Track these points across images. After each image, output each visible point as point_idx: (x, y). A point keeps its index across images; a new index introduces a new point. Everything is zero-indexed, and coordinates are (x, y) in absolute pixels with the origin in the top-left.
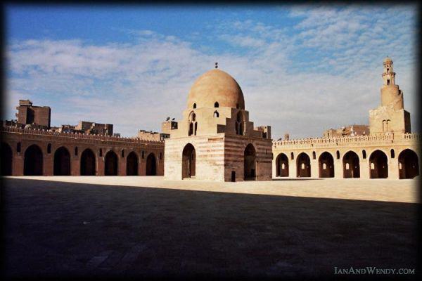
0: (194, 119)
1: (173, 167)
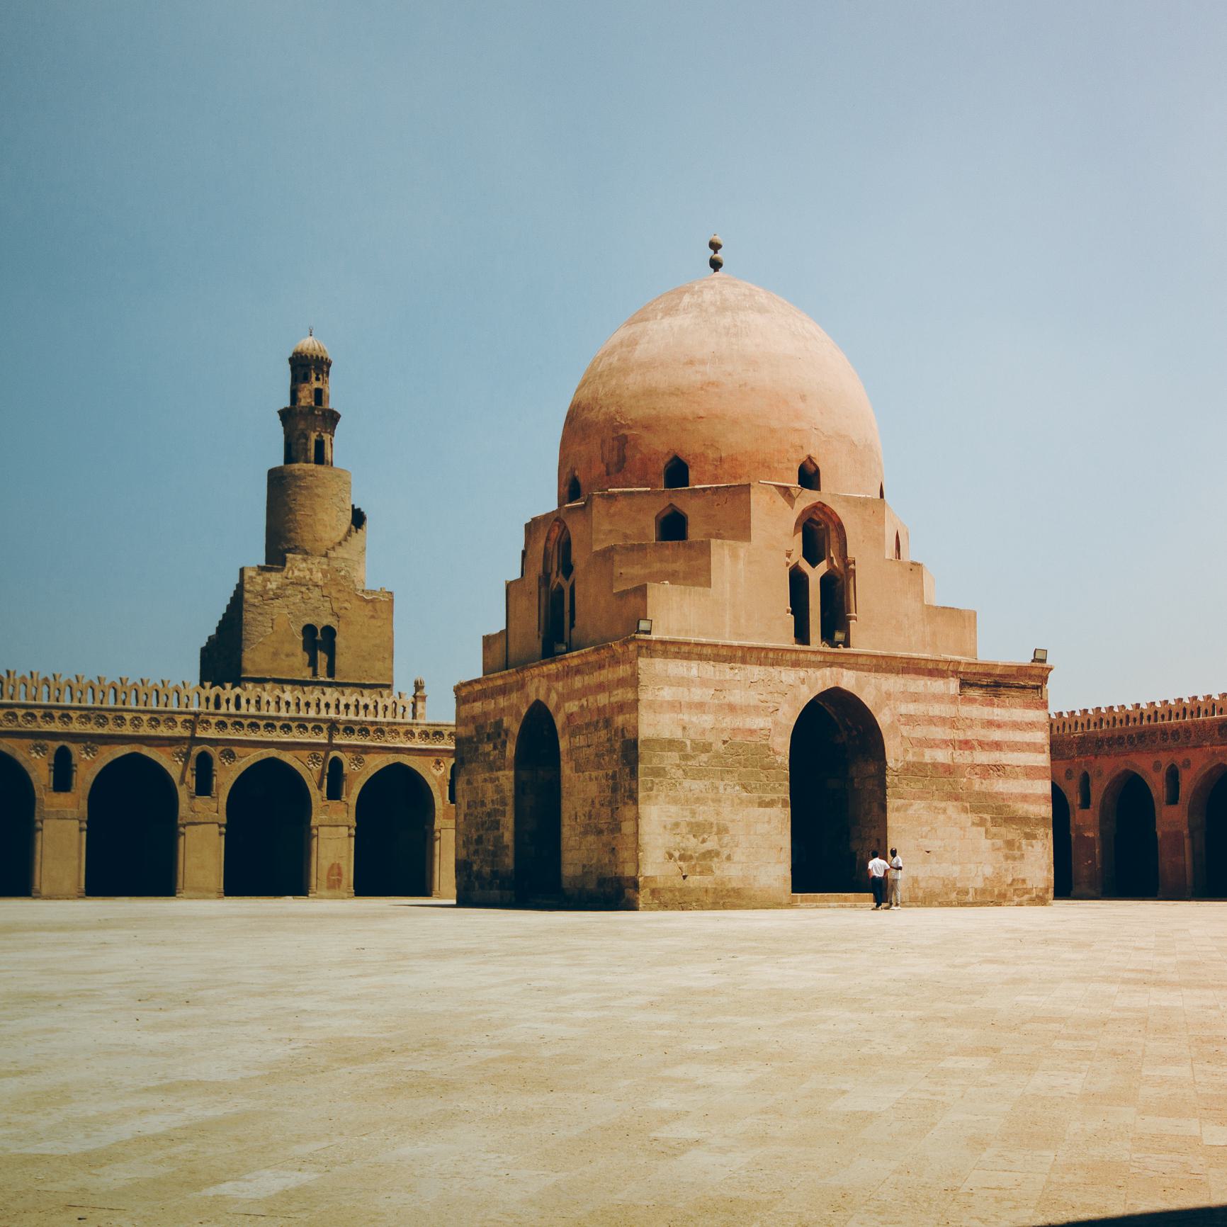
0: (813, 552)
1: (722, 830)
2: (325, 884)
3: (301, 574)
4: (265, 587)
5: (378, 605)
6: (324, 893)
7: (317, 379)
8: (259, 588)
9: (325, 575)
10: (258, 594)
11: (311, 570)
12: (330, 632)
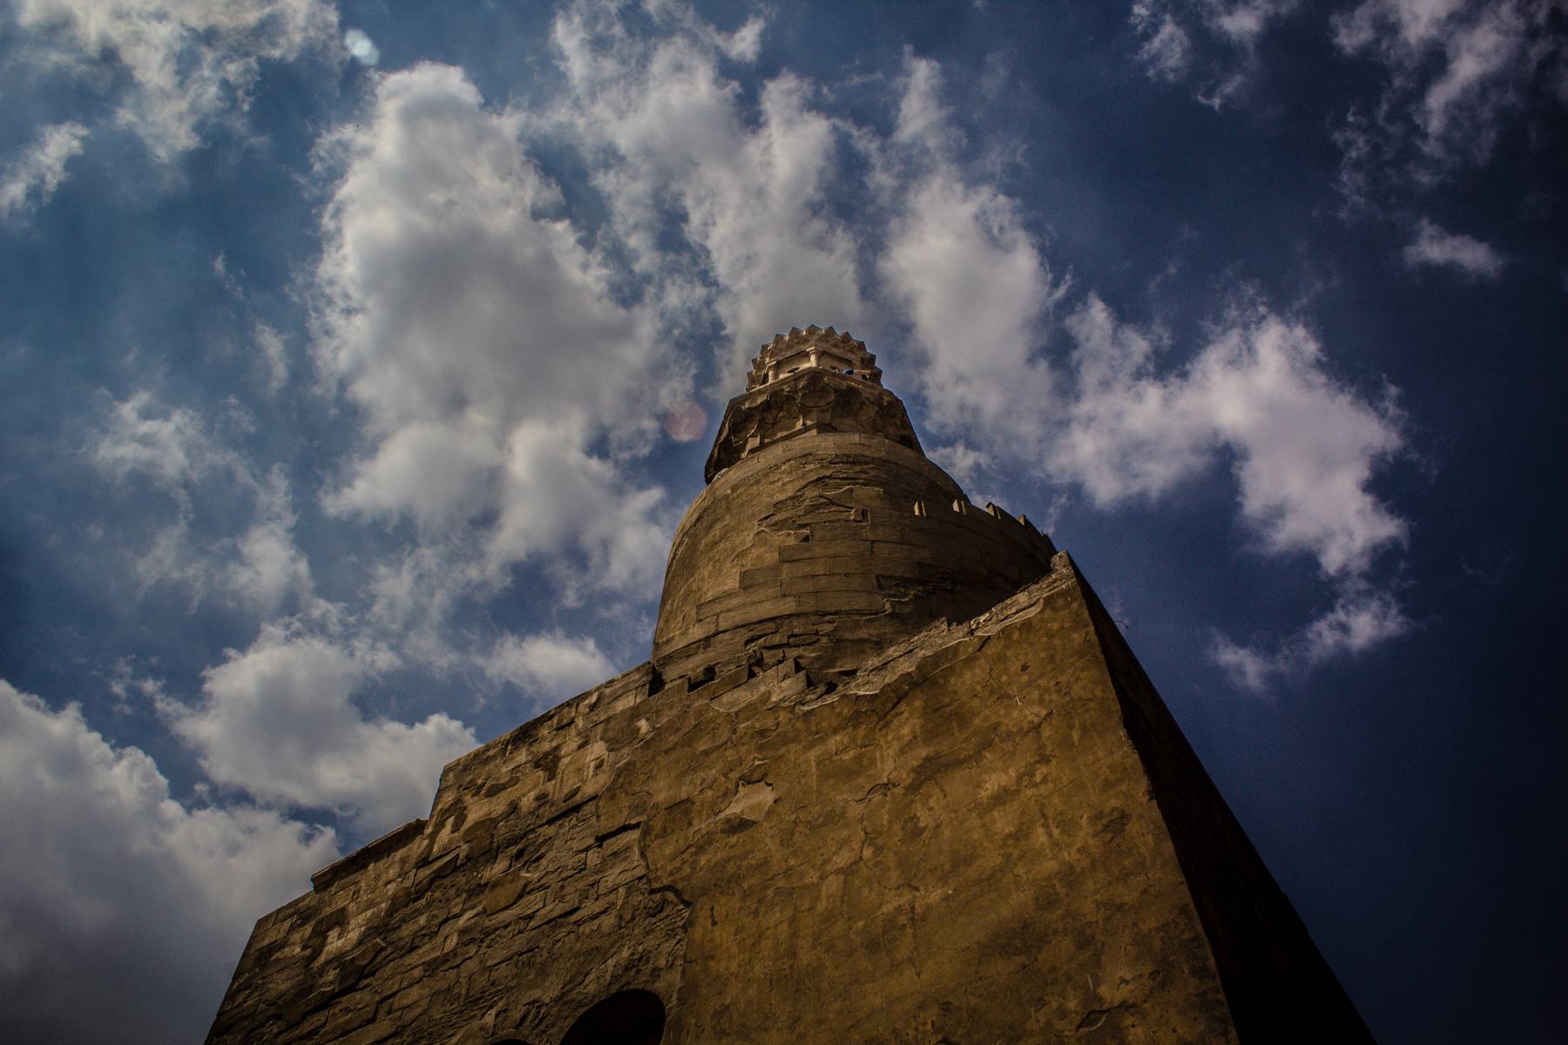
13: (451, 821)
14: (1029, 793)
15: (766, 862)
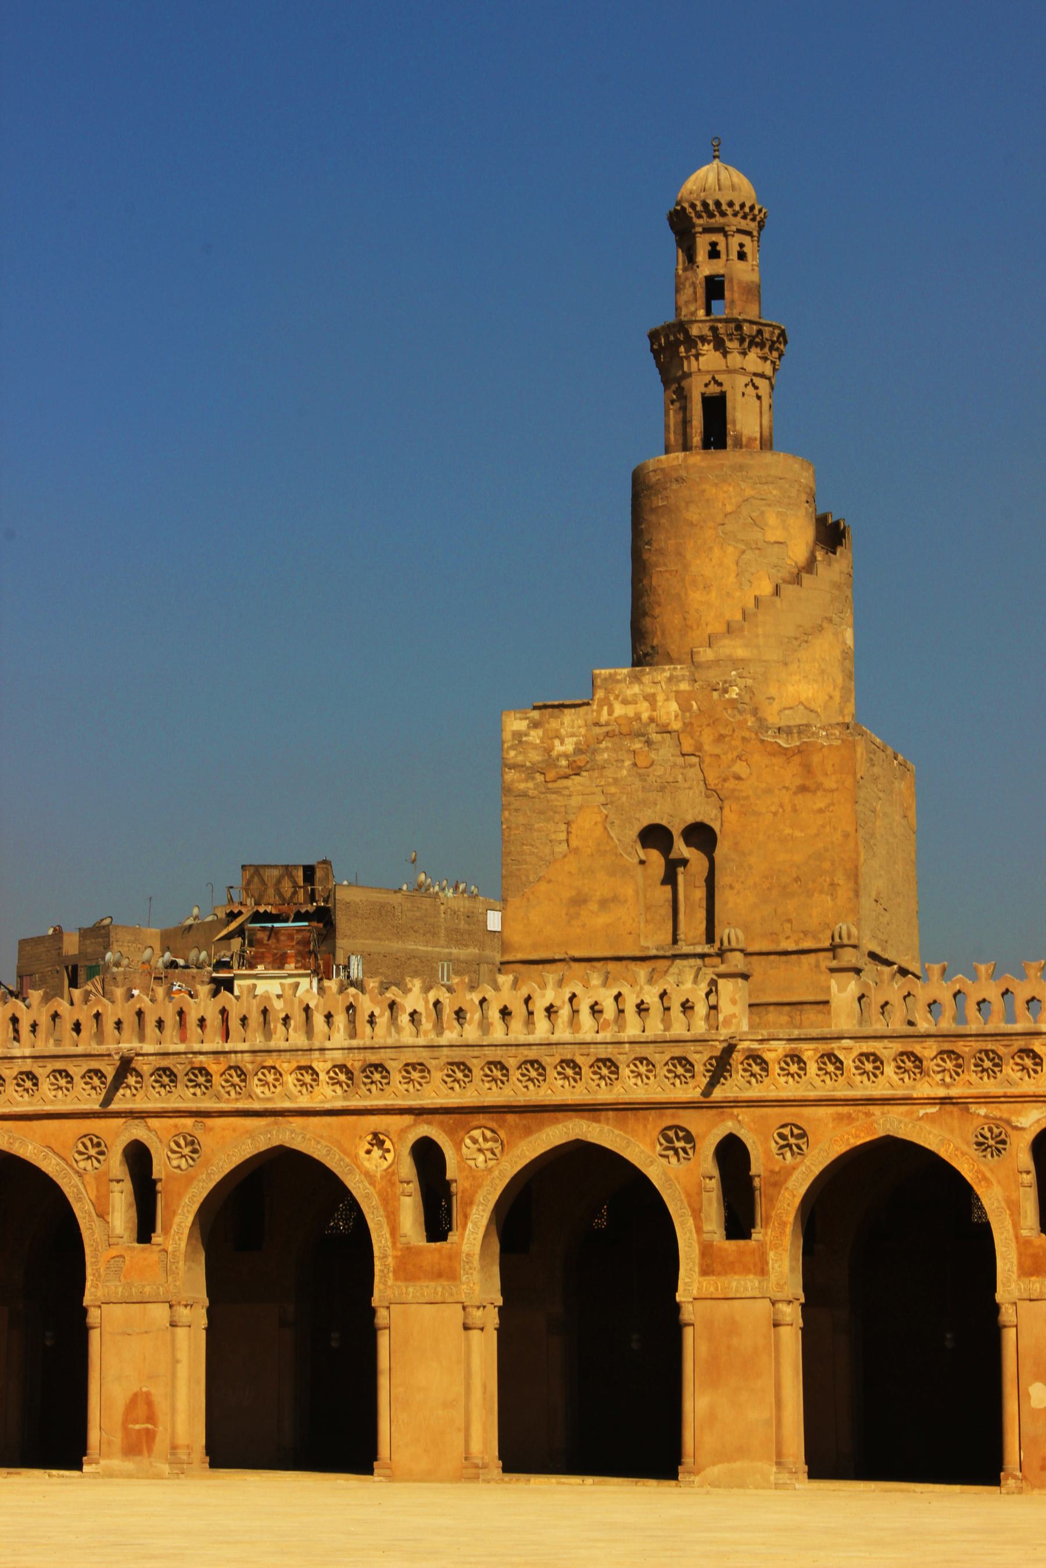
2: (118, 1439)
3: (630, 711)
4: (548, 751)
5: (816, 759)
6: (116, 1463)
7: (714, 253)
8: (535, 756)
9: (685, 708)
10: (531, 771)
11: (651, 699)
12: (701, 836)
13: (605, 708)
14: (828, 813)
15: (747, 798)
